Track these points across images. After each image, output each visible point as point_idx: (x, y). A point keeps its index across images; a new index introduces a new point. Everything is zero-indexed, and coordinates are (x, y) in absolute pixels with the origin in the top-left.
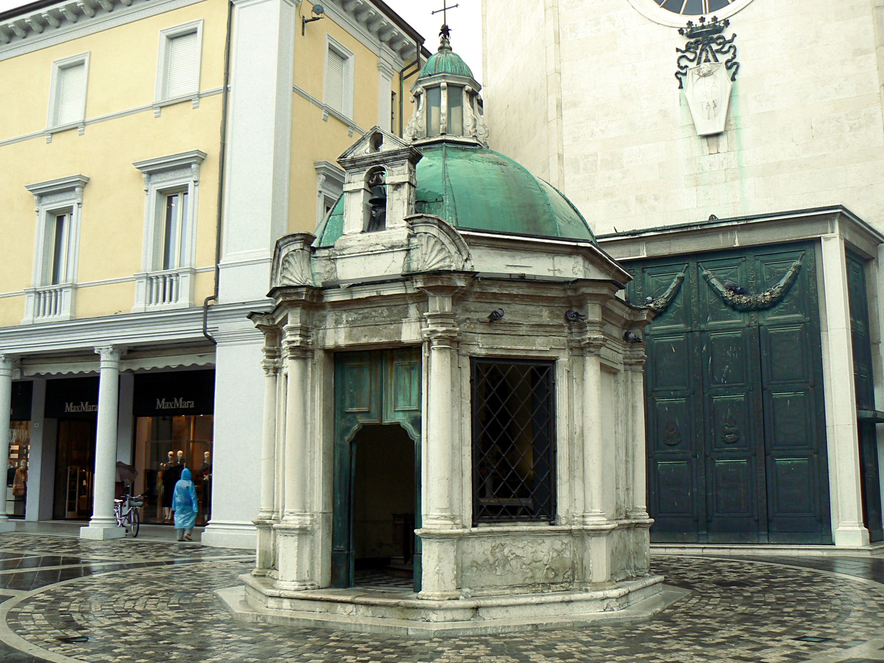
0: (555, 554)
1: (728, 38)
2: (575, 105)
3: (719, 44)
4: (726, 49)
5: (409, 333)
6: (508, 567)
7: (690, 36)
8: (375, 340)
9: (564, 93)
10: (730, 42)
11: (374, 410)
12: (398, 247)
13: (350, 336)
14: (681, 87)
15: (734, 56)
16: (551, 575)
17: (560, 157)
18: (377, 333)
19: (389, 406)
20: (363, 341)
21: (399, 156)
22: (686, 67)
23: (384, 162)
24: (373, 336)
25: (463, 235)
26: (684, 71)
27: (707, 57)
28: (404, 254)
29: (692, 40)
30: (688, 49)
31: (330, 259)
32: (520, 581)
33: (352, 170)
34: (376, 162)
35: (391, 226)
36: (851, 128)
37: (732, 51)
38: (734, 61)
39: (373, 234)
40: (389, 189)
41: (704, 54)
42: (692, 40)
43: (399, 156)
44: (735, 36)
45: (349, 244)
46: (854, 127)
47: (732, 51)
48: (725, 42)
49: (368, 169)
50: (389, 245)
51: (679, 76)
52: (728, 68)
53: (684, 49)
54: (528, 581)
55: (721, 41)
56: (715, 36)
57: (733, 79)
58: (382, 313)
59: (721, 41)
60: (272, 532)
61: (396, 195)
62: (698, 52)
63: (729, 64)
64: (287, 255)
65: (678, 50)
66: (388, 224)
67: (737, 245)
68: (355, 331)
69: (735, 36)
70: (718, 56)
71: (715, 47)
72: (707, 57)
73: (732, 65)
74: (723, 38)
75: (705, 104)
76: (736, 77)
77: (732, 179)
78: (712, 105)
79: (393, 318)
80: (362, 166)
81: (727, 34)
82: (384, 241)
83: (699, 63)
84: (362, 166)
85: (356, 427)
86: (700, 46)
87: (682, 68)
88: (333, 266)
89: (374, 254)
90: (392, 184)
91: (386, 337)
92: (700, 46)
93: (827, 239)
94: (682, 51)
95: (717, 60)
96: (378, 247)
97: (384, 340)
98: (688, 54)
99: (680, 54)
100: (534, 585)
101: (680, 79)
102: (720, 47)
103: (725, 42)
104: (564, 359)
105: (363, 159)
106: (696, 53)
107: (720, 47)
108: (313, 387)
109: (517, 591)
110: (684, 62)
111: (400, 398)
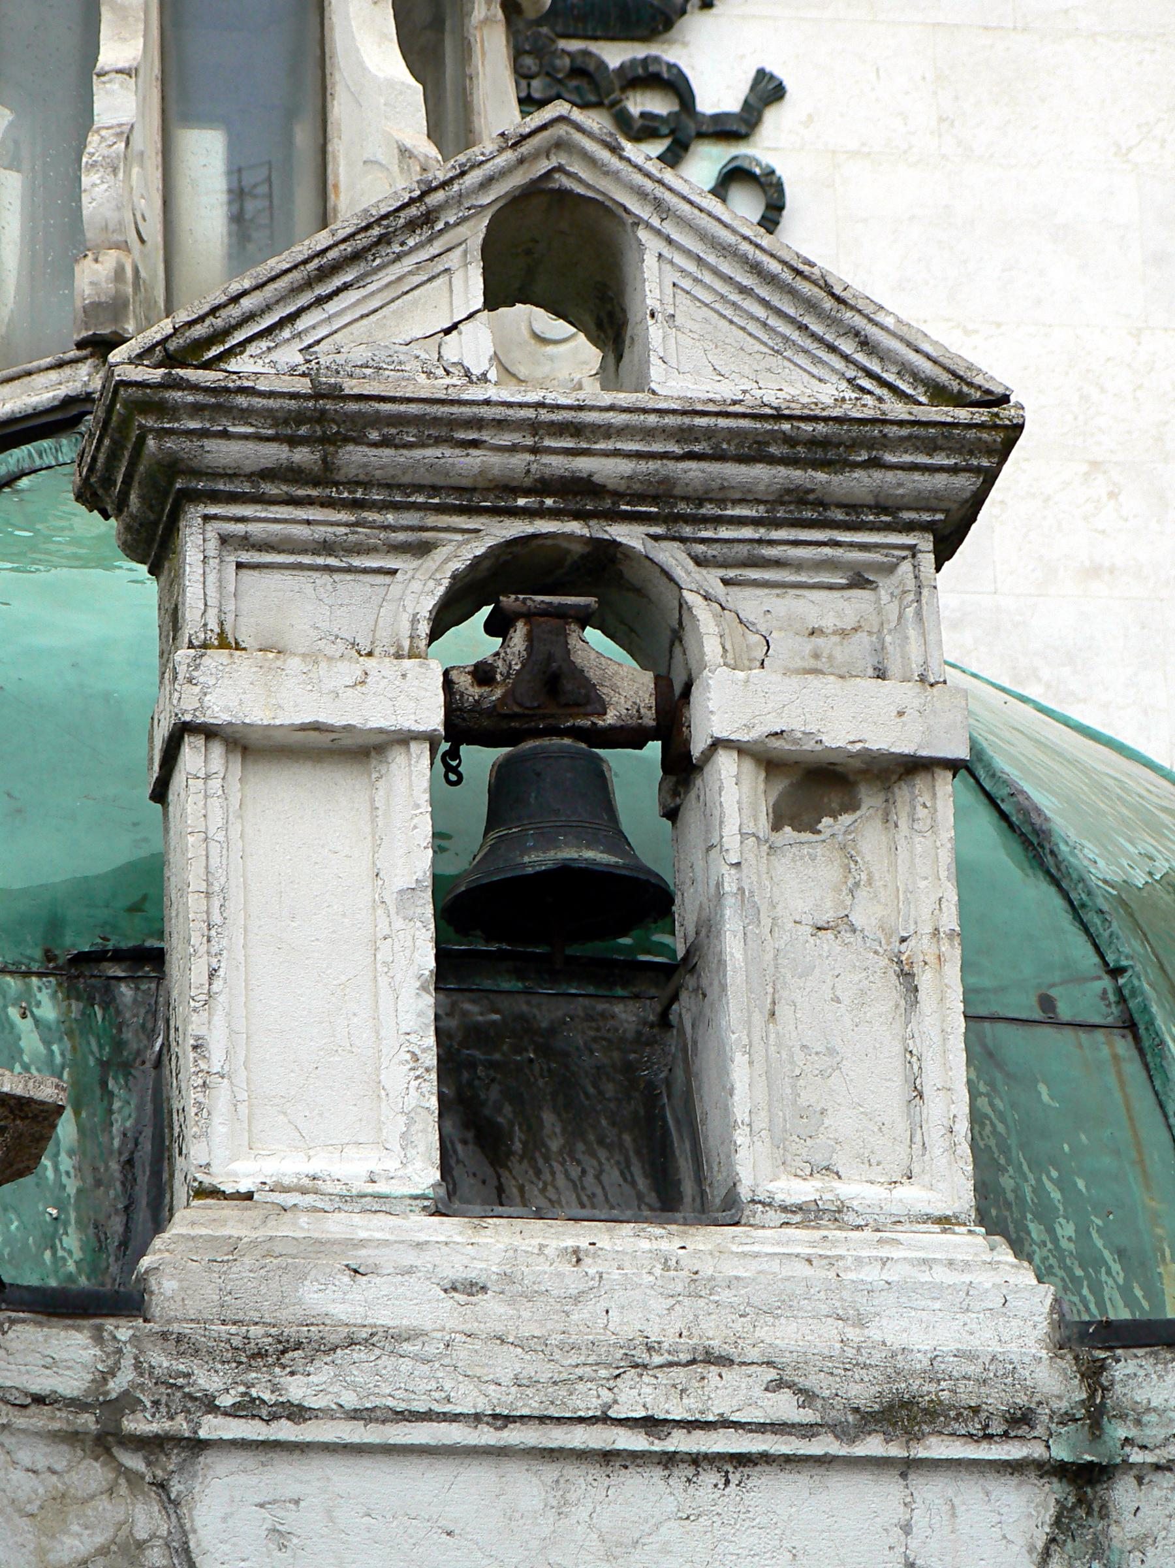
1: (718, 93)
10: (730, 130)
12: (973, 1420)
21: (859, 483)
23: (663, 505)
28: (1025, 1510)
31: (106, 1442)
33: (263, 520)
34: (579, 495)
35: (801, 1191)
39: (449, 1228)
40: (734, 795)
43: (859, 483)
44: (767, 91)
45: (333, 1301)
48: (683, 132)
49: (466, 545)
50: (862, 1392)
55: (658, 105)
56: (615, 55)
59: (658, 105)
66: (752, 1162)
69: (767, 91)
74: (676, 85)
80: (400, 493)
82: (785, 1336)
84: (400, 493)
88: (146, 1518)
89: (665, 1451)
90: (769, 759)
96: (726, 1394)
105: (446, 423)
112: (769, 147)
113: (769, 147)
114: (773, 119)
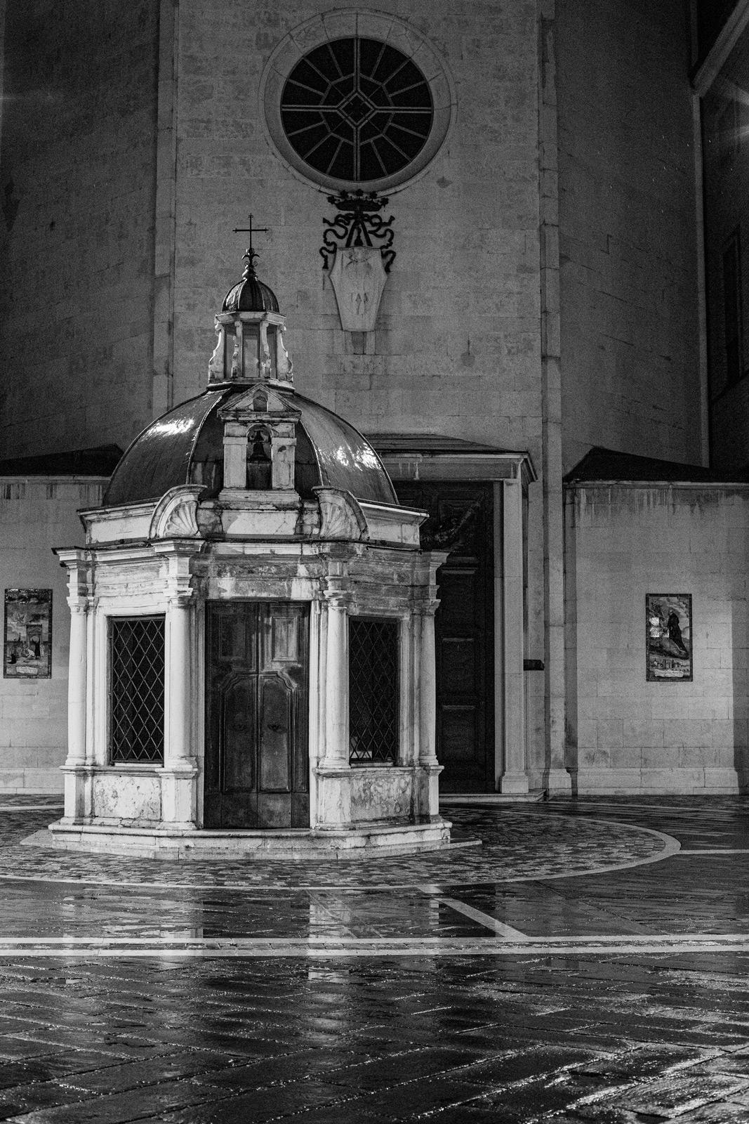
0: (401, 792)
1: (386, 220)
2: (192, 262)
3: (374, 225)
4: (381, 232)
5: (300, 590)
6: (373, 803)
7: (339, 206)
8: (264, 595)
9: (180, 245)
13: (237, 588)
14: (325, 267)
15: (391, 244)
16: (398, 810)
17: (171, 325)
18: (265, 589)
20: (251, 594)
22: (334, 243)
24: (260, 591)
25: (364, 508)
26: (331, 248)
27: (359, 237)
29: (344, 213)
30: (337, 221)
32: (379, 816)
36: (509, 352)
37: (389, 235)
38: (390, 248)
41: (356, 232)
42: (344, 213)
44: (392, 218)
46: (513, 351)
47: (389, 235)
48: (381, 224)
51: (325, 253)
52: (384, 256)
53: (332, 221)
54: (385, 816)
55: (377, 221)
57: (387, 270)
58: (269, 569)
60: (90, 778)
61: (281, 456)
62: (349, 227)
63: (385, 250)
64: (179, 506)
65: (325, 221)
67: (417, 478)
68: (241, 584)
69: (392, 218)
70: (371, 236)
71: (369, 227)
72: (359, 237)
73: (389, 256)
74: (379, 218)
75: (355, 297)
76: (392, 268)
77: (378, 388)
78: (363, 298)
79: (281, 576)
81: (385, 214)
83: (348, 245)
86: (352, 222)
87: (329, 244)
91: (275, 593)
92: (352, 222)
93: (509, 484)
94: (331, 224)
95: (370, 244)
97: (273, 595)
98: (337, 228)
99: (327, 227)
100: (388, 819)
101: (326, 258)
102: (375, 228)
103: (381, 224)
104: (406, 618)
106: (346, 229)
107: (375, 228)
108: (197, 635)
109: (380, 823)
110: (331, 238)
111: (277, 649)
112: (392, 227)
113: (392, 227)
114: (394, 223)
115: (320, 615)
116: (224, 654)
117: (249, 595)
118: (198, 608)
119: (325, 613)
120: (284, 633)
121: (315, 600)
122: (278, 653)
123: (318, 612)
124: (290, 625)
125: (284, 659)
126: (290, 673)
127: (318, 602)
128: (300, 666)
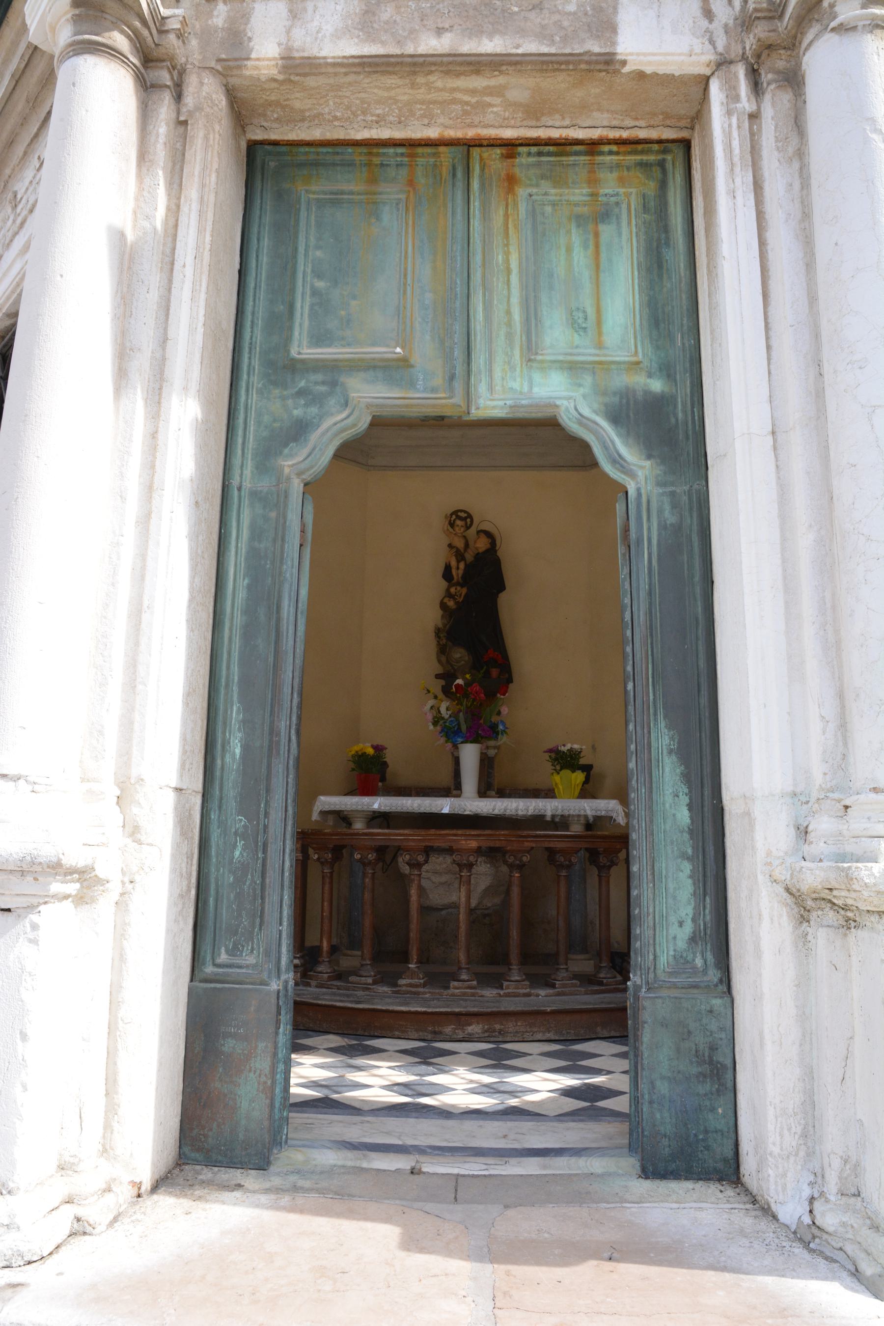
11: (425, 354)
19: (500, 342)
24: (477, 32)
85: (336, 425)
91: (542, 35)
115: (754, 117)
116: (319, 338)
117: (422, 49)
118: (189, 100)
119: (786, 97)
120: (581, 258)
121: (723, 63)
122: (557, 336)
123: (746, 103)
124: (606, 231)
125: (588, 354)
126: (616, 417)
127: (741, 71)
128: (657, 385)
